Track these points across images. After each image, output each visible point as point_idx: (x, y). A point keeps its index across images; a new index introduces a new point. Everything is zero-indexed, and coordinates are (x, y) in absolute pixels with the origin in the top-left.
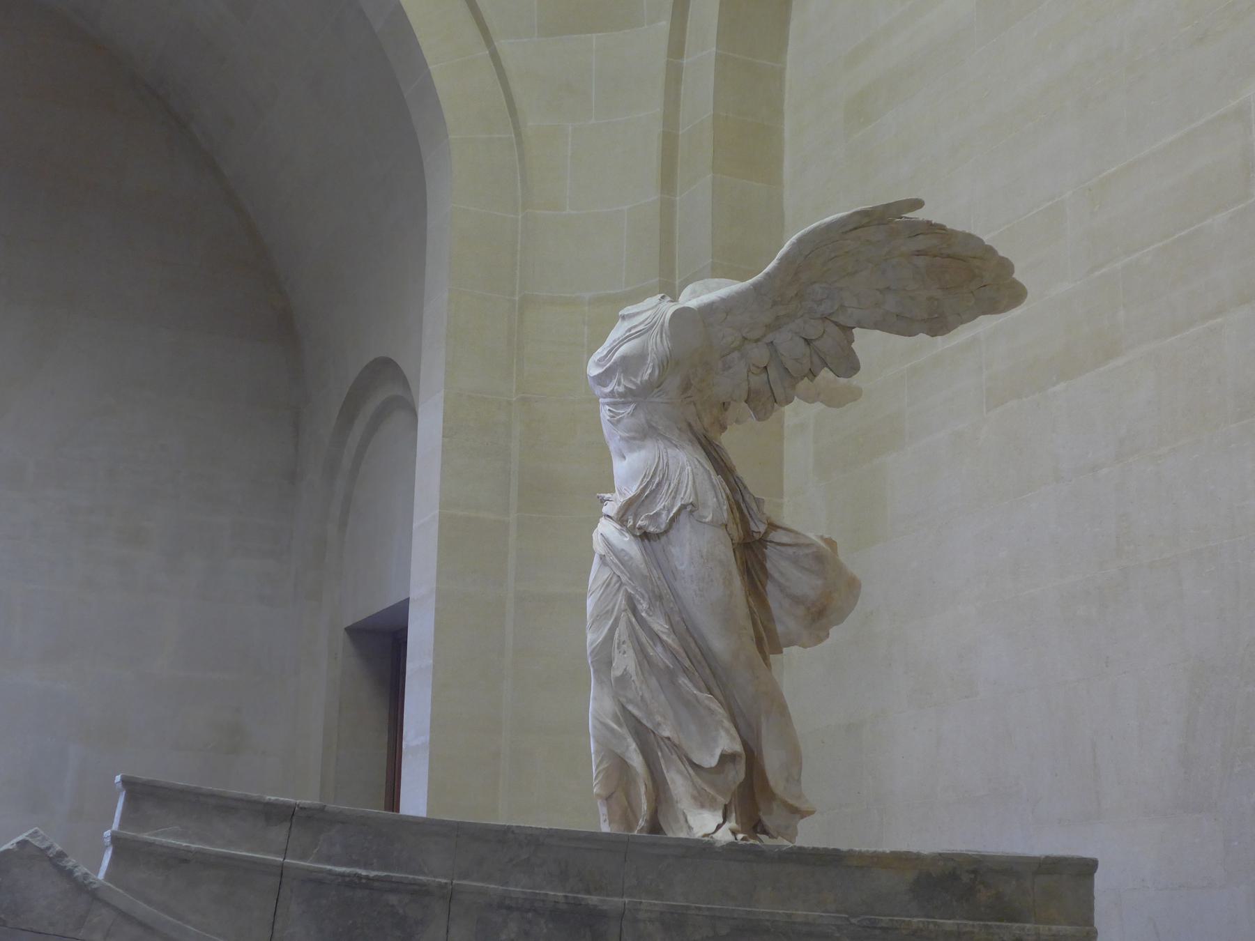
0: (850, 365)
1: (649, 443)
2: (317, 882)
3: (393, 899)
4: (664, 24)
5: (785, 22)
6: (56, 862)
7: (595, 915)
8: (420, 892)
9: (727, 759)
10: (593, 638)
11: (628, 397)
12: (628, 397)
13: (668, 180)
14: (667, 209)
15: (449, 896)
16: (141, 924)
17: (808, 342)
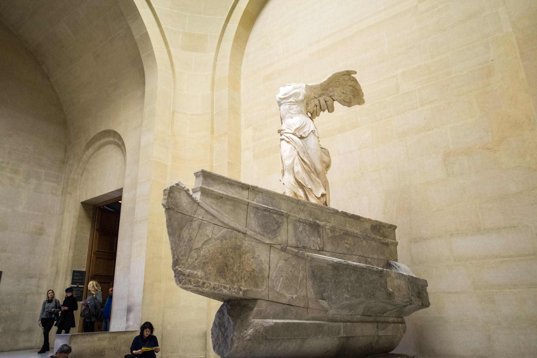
0: (331, 109)
1: (300, 115)
2: (257, 208)
3: (275, 216)
4: (213, 54)
5: (242, 59)
6: (187, 191)
7: (318, 226)
8: (281, 214)
9: (323, 195)
10: (288, 162)
11: (297, 102)
12: (297, 102)
13: (213, 89)
14: (213, 95)
15: (288, 216)
16: (212, 215)
17: (326, 101)
